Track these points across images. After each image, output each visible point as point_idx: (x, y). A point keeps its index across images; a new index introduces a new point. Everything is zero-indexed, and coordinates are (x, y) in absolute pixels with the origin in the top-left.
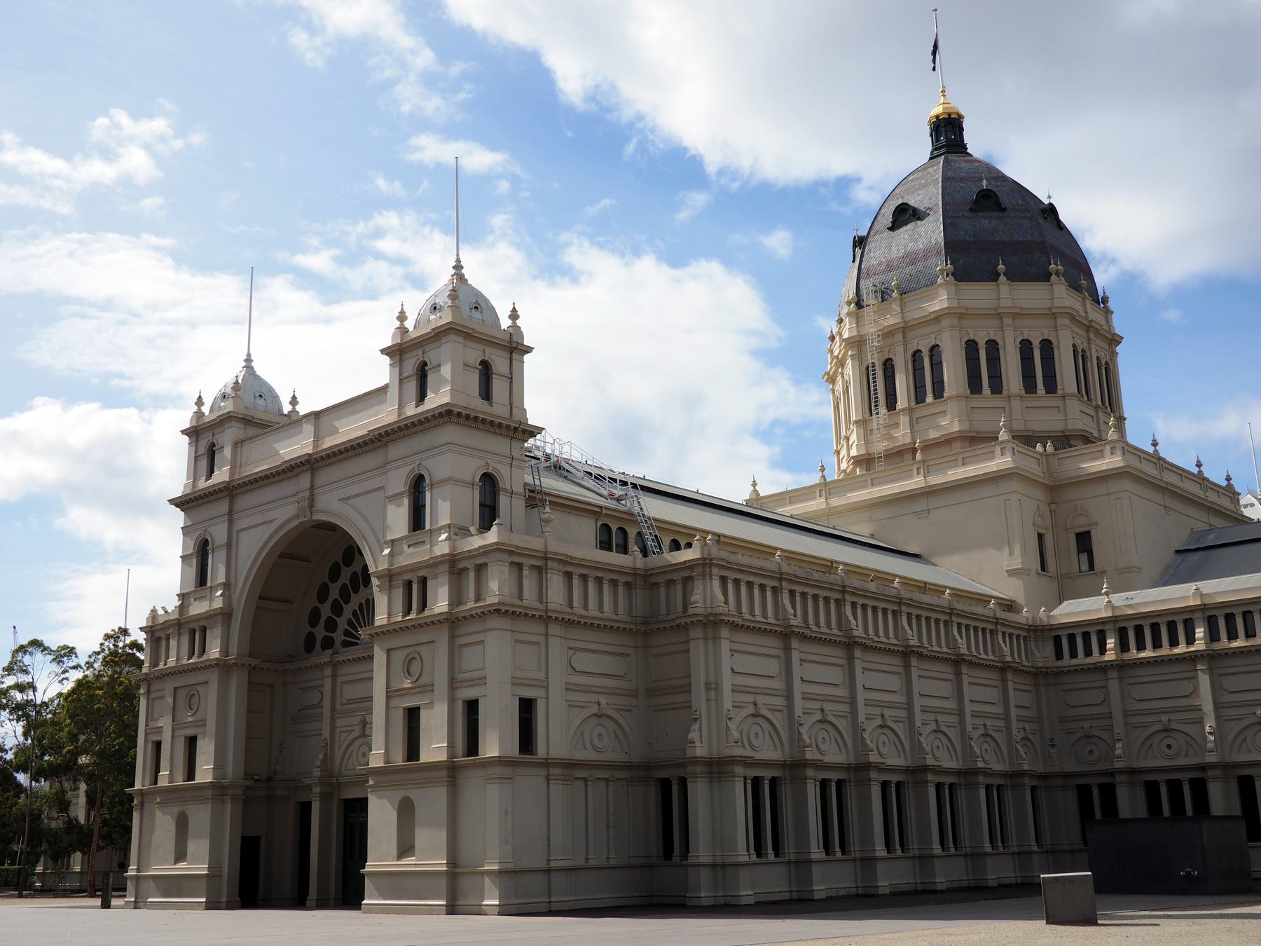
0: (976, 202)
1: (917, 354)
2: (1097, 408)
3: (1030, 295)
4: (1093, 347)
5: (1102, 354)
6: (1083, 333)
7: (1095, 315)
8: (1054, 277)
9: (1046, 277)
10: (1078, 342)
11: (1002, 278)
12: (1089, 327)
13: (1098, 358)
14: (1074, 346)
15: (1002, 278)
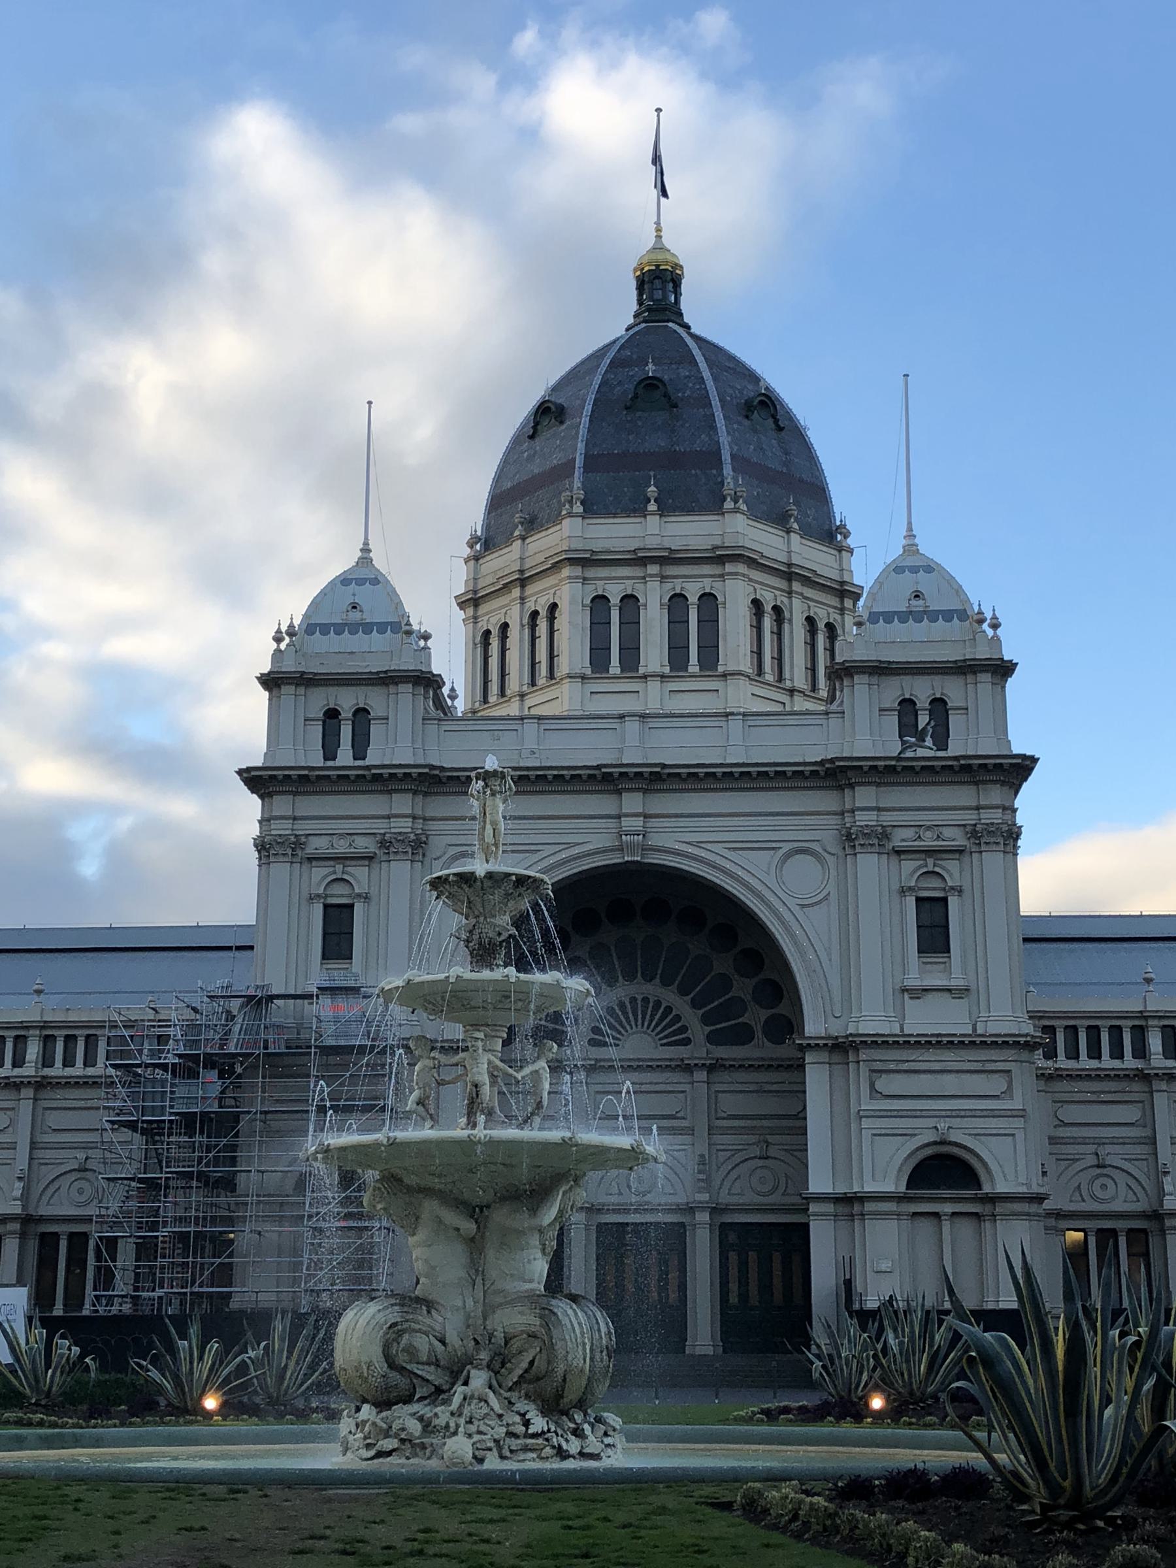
0: (636, 396)
1: (535, 614)
2: (791, 692)
3: (690, 531)
4: (796, 602)
5: (823, 616)
6: (783, 584)
7: (810, 555)
8: (729, 504)
9: (714, 504)
10: (769, 599)
11: (652, 507)
12: (789, 574)
13: (810, 620)
14: (757, 604)
15: (652, 507)
